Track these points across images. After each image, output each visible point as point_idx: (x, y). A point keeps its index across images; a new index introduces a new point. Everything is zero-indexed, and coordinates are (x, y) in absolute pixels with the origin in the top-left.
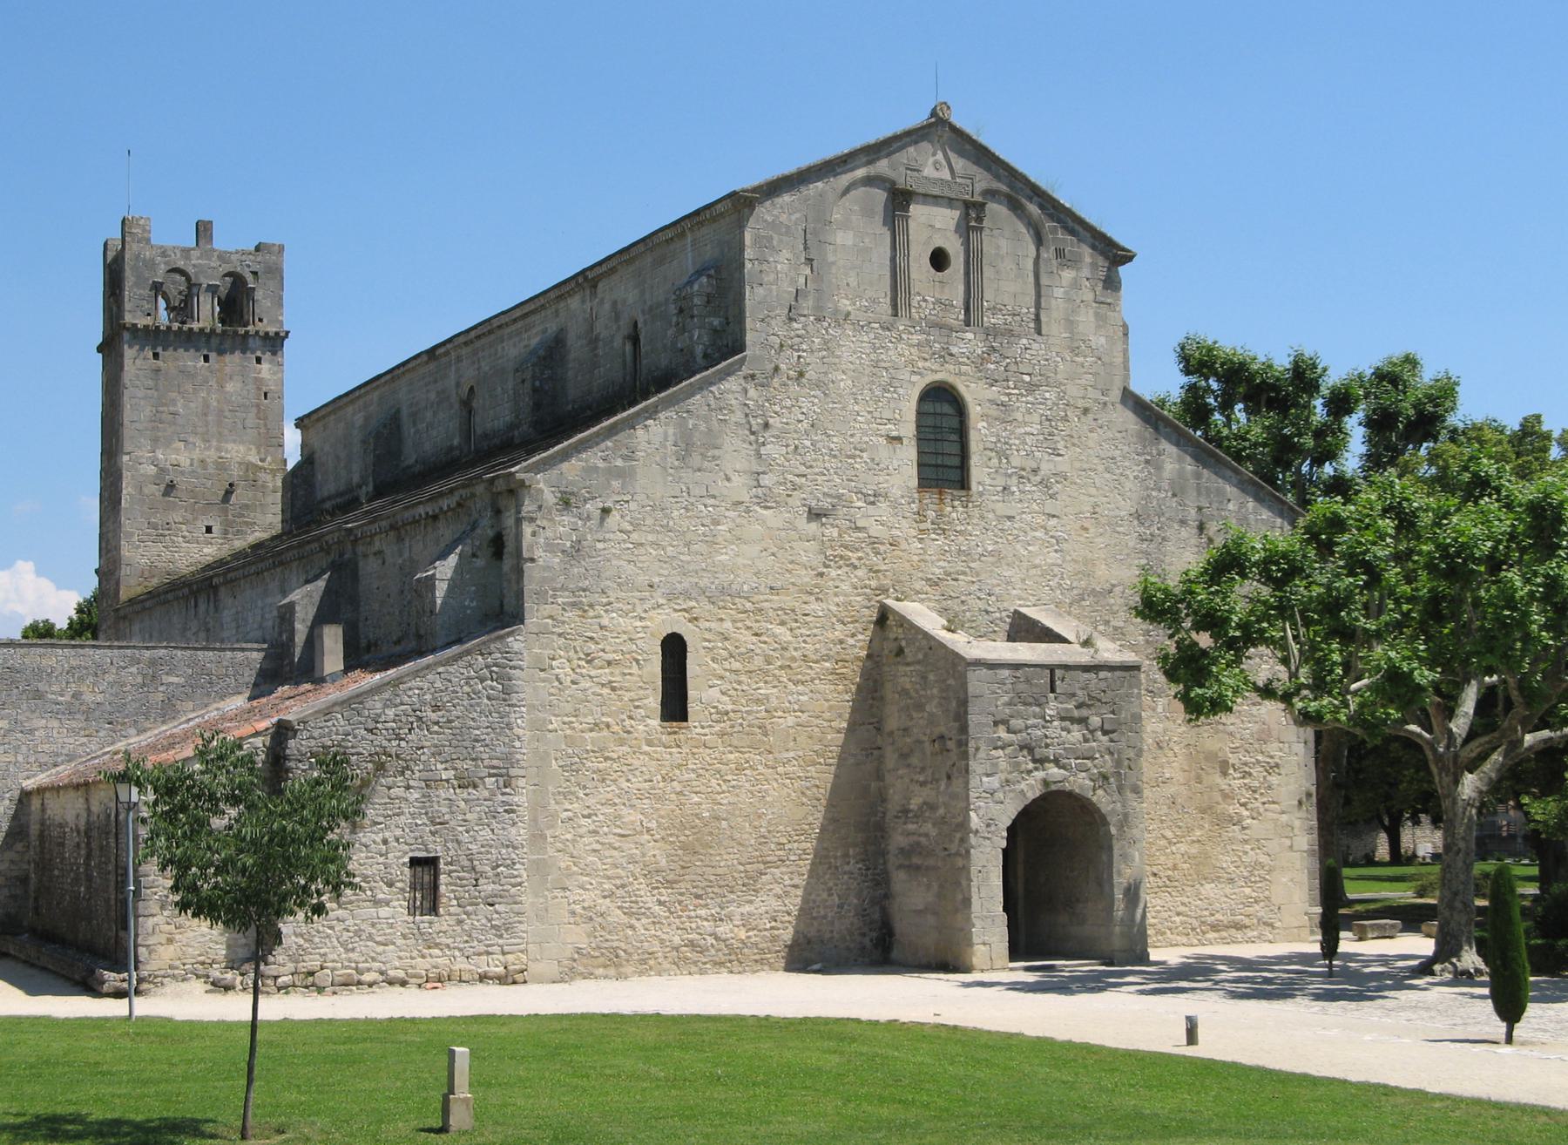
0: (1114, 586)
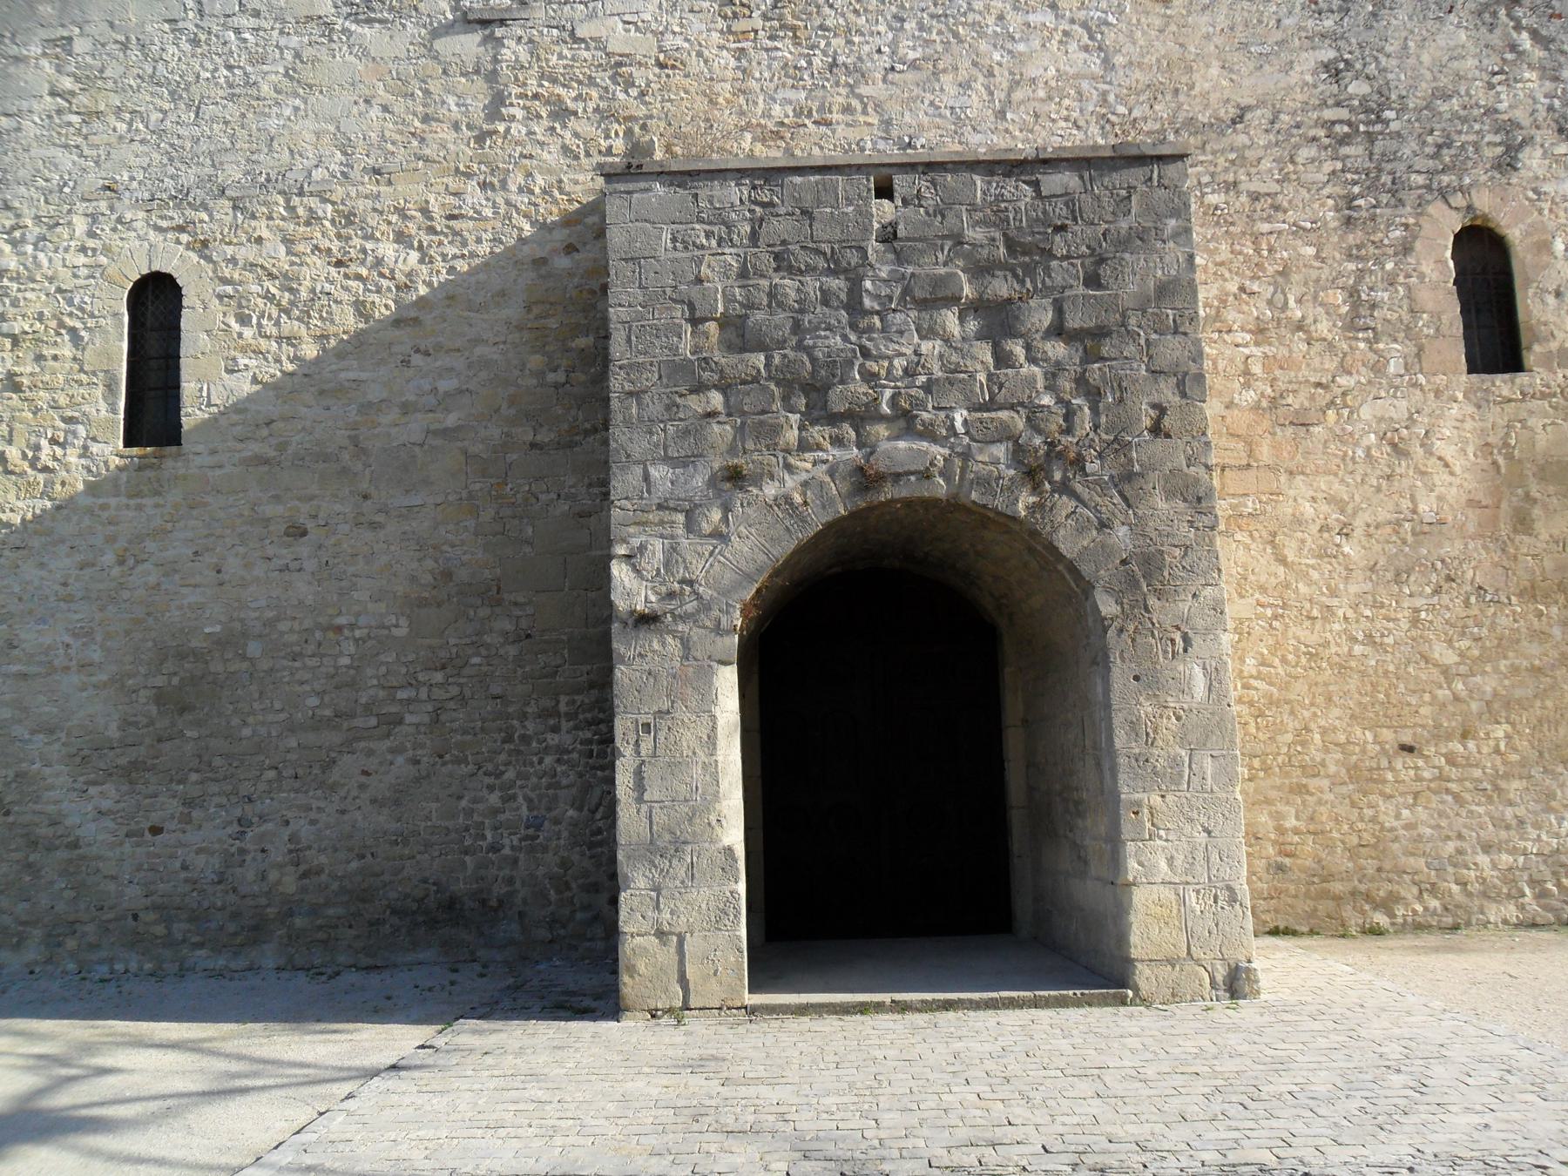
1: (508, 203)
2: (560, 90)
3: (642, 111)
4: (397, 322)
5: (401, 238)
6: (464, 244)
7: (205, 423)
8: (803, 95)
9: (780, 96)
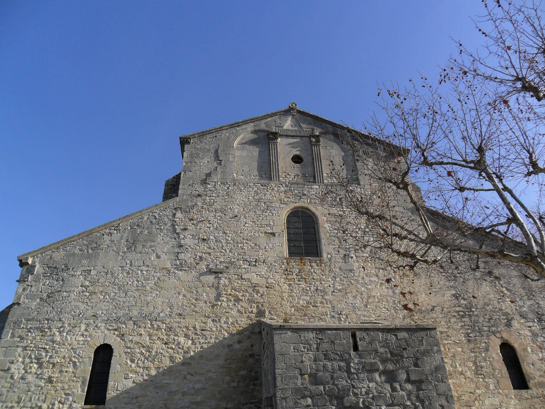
0: (434, 307)
1: (221, 326)
2: (237, 293)
3: (262, 301)
4: (183, 364)
5: (186, 336)
6: (206, 339)
7: (114, 397)
8: (309, 298)
9: (302, 298)
